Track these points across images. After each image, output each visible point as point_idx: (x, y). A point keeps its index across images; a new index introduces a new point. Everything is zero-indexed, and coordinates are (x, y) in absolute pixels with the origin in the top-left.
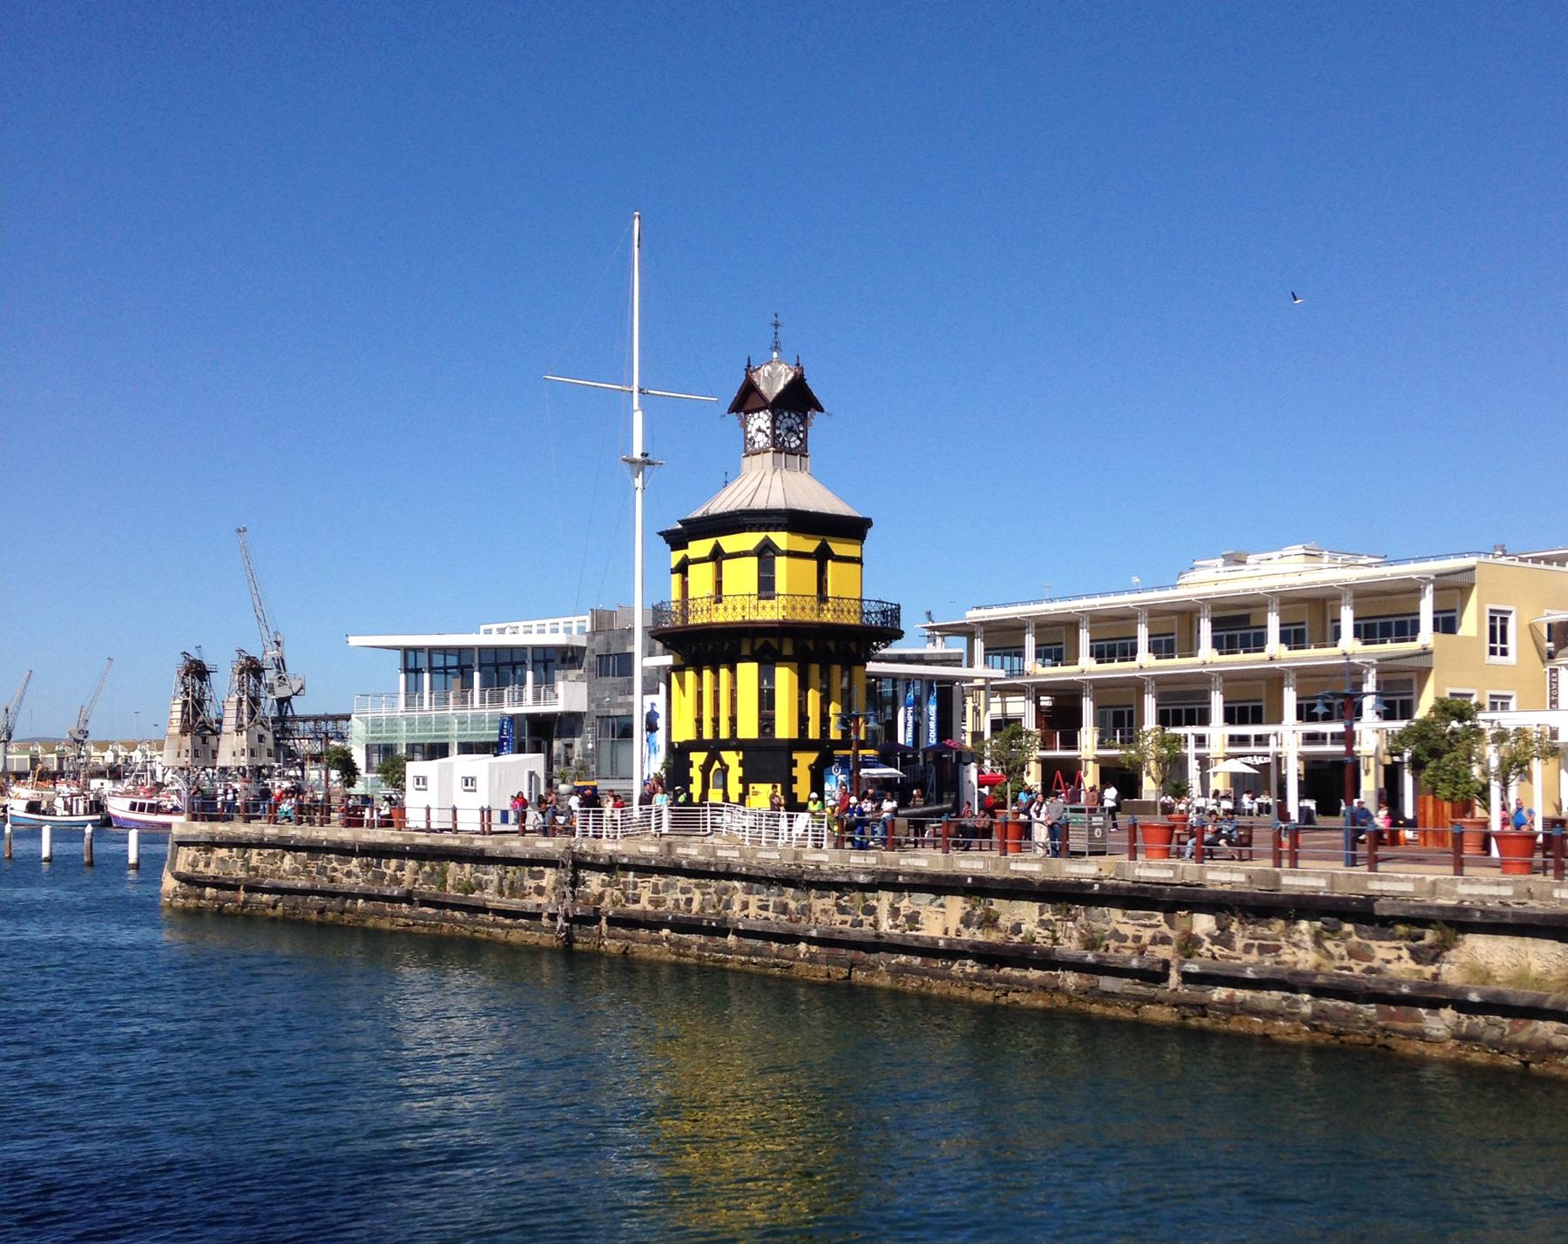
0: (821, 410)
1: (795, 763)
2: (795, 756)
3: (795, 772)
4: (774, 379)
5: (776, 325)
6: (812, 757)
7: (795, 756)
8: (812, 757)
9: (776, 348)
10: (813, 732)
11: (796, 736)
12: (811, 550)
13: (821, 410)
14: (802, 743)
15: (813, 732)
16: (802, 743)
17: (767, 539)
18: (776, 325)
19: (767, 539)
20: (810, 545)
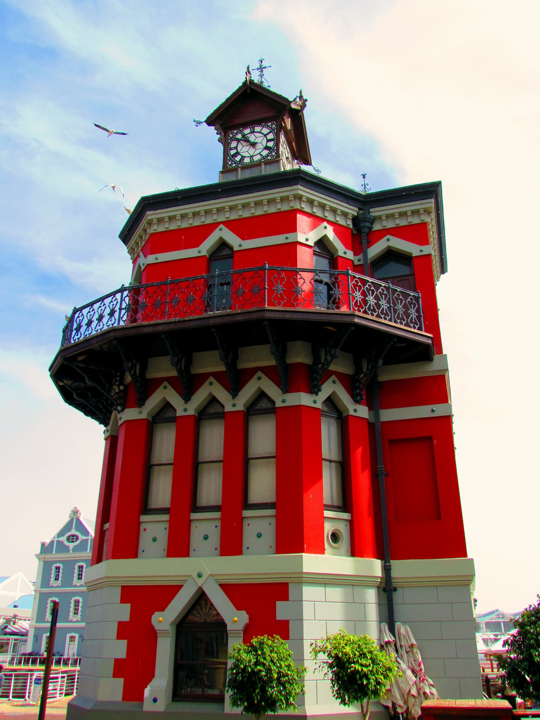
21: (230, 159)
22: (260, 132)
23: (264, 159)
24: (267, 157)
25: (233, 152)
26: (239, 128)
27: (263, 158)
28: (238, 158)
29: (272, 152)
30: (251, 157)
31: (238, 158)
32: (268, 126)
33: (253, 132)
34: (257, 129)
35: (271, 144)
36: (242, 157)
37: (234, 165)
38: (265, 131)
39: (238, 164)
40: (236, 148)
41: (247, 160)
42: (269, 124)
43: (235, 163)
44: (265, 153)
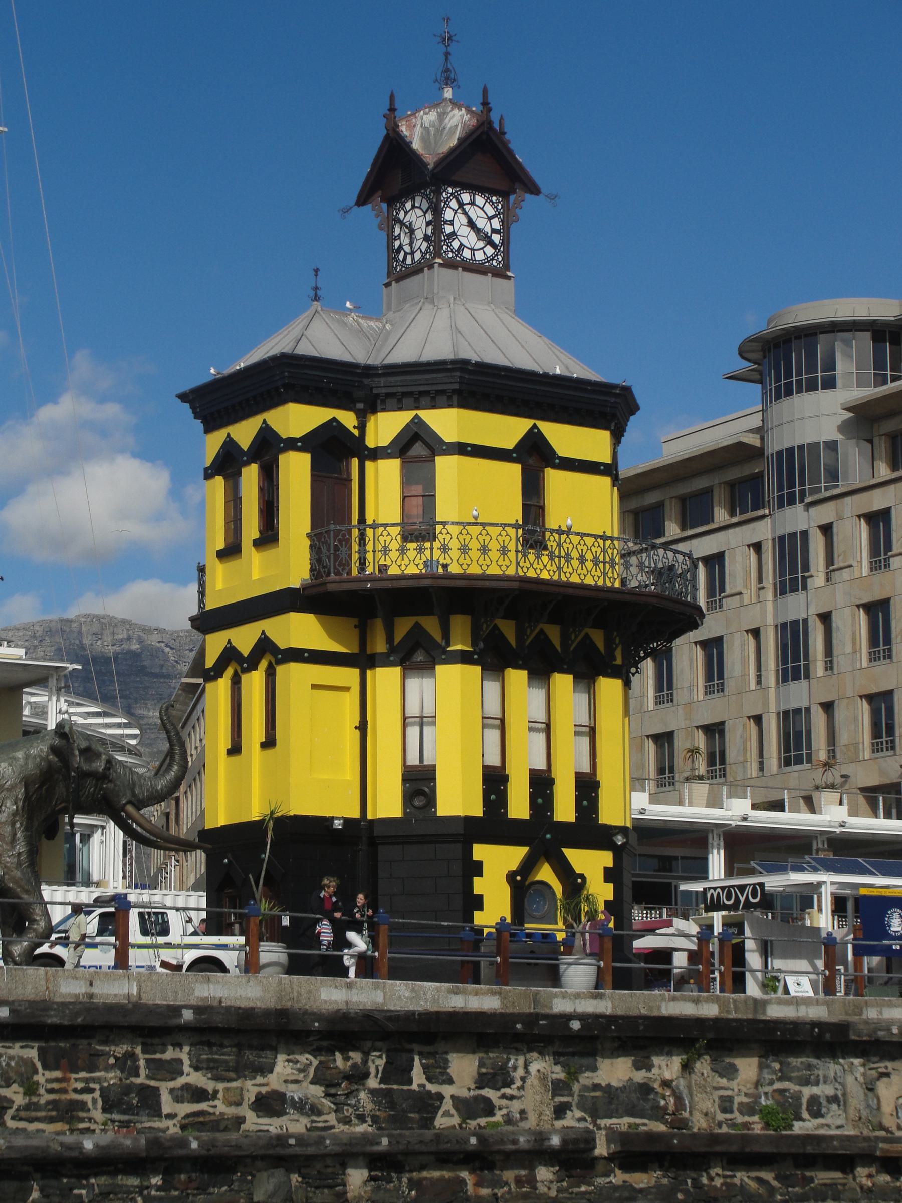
0: (535, 190)
1: (477, 869)
2: (480, 851)
3: (479, 886)
4: (436, 128)
5: (447, 40)
6: (512, 856)
7: (480, 851)
8: (512, 856)
9: (448, 79)
10: (519, 806)
11: (477, 810)
12: (509, 443)
13: (535, 190)
14: (493, 825)
15: (519, 806)
16: (493, 825)
17: (417, 422)
18: (447, 40)
19: (417, 422)
20: (507, 430)
21: (445, 240)
22: (482, 209)
23: (488, 261)
24: (493, 259)
25: (448, 229)
26: (455, 187)
27: (489, 259)
28: (455, 244)
29: (497, 255)
30: (472, 249)
31: (455, 244)
32: (491, 201)
33: (472, 203)
34: (479, 200)
35: (496, 238)
36: (461, 244)
37: (450, 255)
38: (491, 211)
39: (456, 255)
40: (451, 223)
41: (467, 254)
42: (494, 199)
43: (452, 251)
44: (490, 250)
